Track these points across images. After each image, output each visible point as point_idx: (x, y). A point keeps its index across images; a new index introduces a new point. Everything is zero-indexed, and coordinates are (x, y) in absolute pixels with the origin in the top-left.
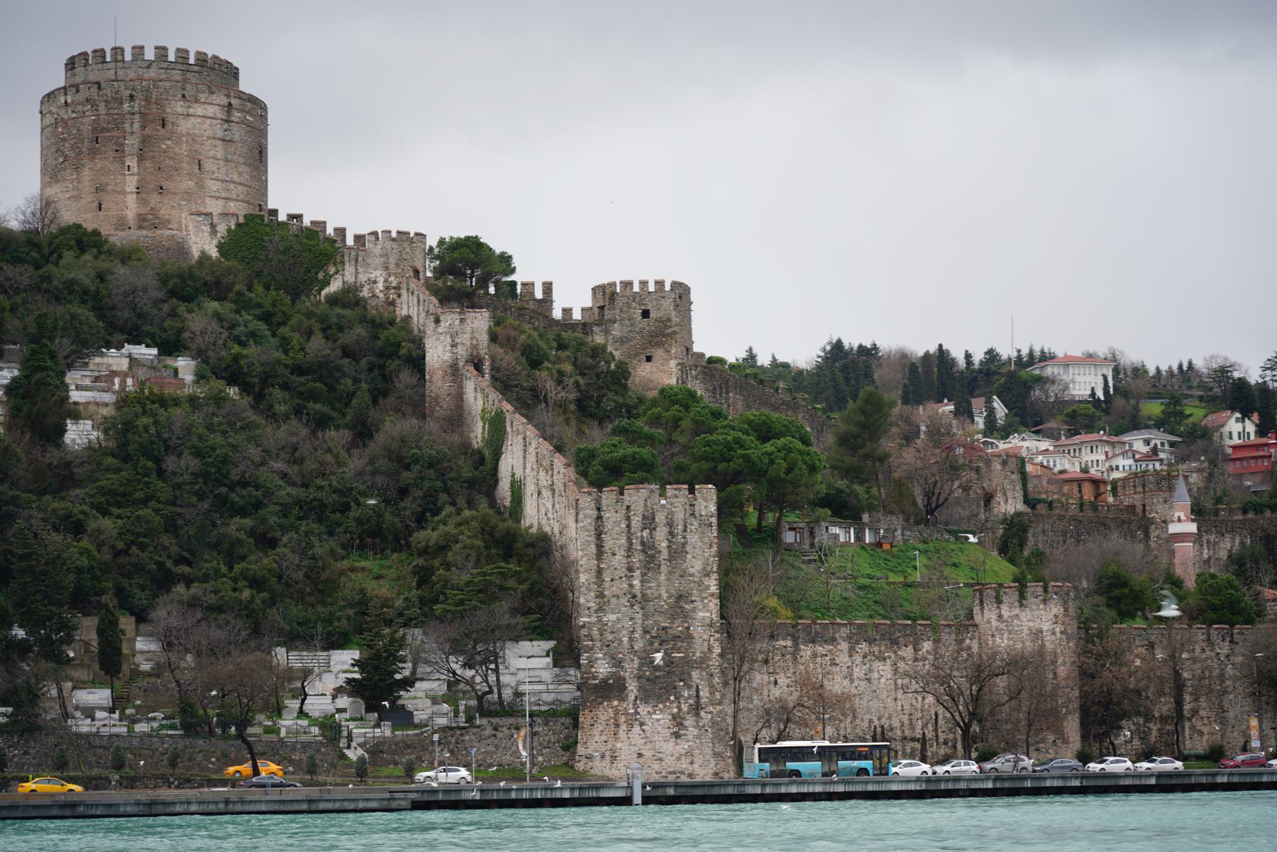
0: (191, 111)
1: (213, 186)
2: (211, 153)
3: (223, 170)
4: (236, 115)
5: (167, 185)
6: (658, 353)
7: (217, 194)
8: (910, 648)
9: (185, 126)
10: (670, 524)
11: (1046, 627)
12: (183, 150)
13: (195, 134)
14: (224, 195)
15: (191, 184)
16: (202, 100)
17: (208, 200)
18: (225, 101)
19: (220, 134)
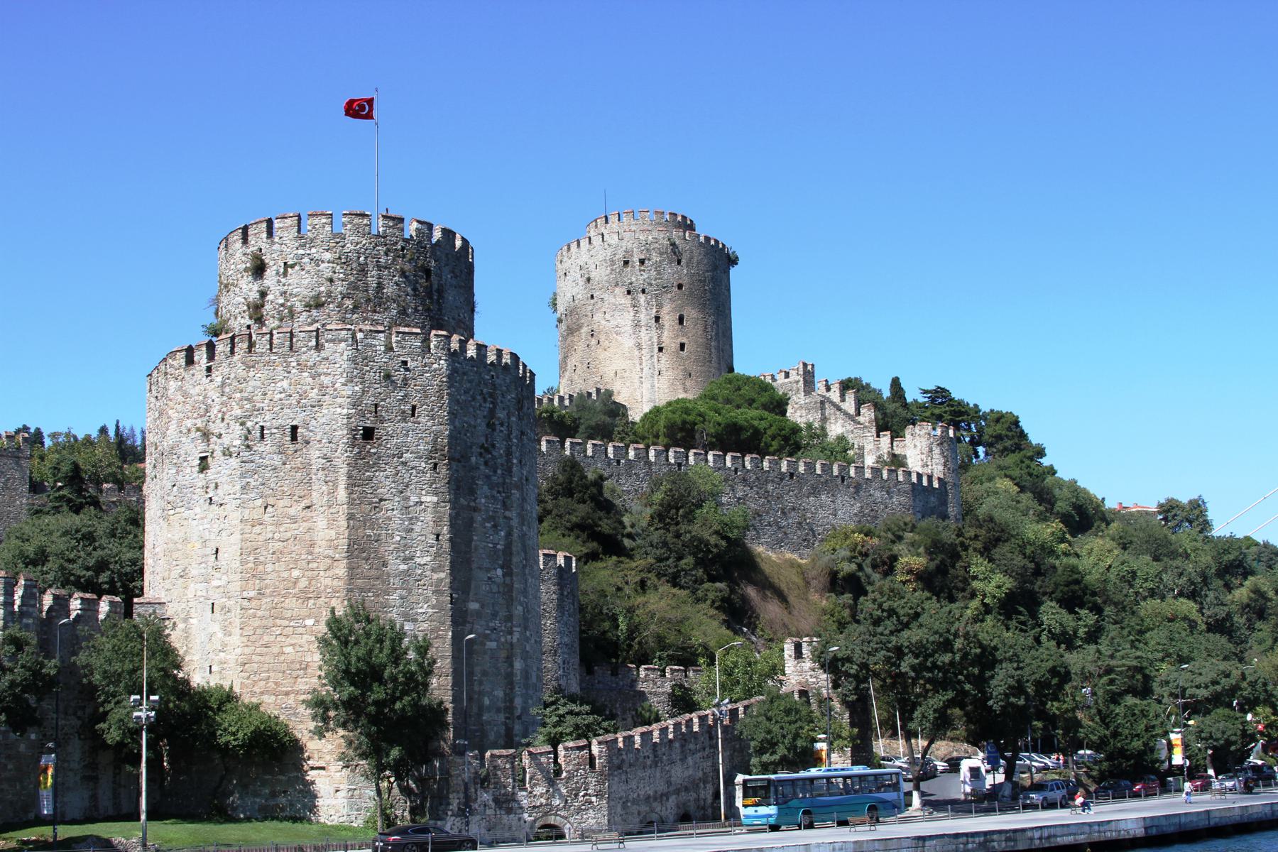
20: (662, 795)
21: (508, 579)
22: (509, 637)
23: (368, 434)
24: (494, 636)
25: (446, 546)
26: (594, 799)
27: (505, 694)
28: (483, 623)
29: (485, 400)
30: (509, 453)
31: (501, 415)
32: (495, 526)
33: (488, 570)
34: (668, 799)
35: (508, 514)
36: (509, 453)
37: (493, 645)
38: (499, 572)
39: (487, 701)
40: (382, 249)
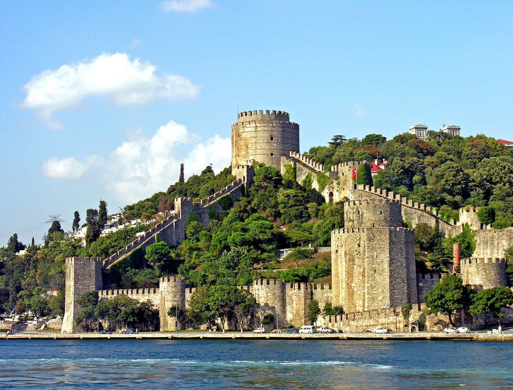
0: (245, 131)
1: (251, 151)
2: (250, 142)
3: (254, 146)
4: (259, 129)
5: (240, 154)
6: (345, 187)
7: (252, 154)
8: (147, 296)
9: (243, 135)
10: (69, 268)
11: (163, 290)
12: (242, 143)
13: (246, 137)
14: (254, 154)
15: (245, 152)
16: (248, 127)
17: (249, 156)
18: (254, 125)
19: (253, 136)
20: (373, 325)
21: (364, 278)
22: (364, 291)
23: (337, 251)
24: (359, 291)
25: (347, 273)
26: (347, 325)
27: (363, 303)
28: (356, 288)
29: (357, 241)
30: (364, 251)
31: (362, 242)
32: (360, 267)
33: (358, 277)
34: (377, 326)
35: (364, 264)
36: (364, 251)
37: (359, 293)
38: (361, 277)
39: (357, 305)
40: (350, 209)
